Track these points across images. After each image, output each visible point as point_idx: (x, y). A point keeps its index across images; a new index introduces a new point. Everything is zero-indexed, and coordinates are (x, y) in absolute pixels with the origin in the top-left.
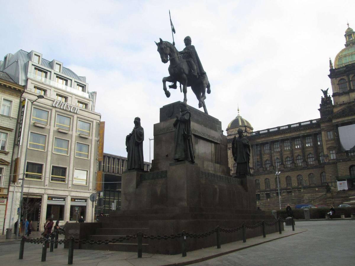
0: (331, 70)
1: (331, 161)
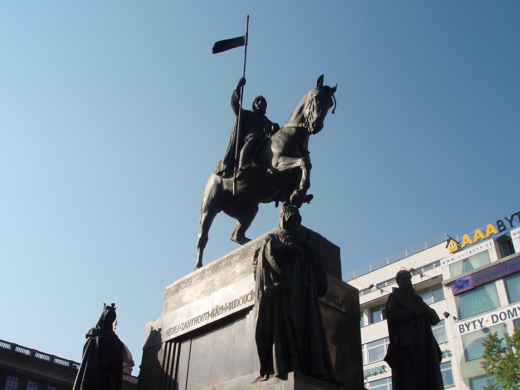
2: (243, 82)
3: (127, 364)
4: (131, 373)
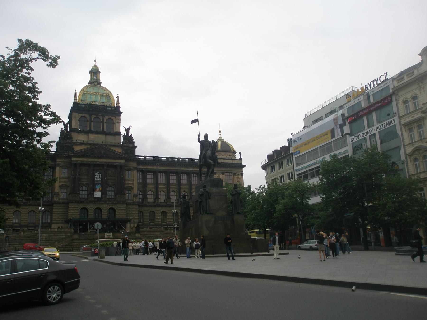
0: (75, 103)
1: (61, 201)
2: (199, 135)
3: (232, 153)
4: (235, 158)
